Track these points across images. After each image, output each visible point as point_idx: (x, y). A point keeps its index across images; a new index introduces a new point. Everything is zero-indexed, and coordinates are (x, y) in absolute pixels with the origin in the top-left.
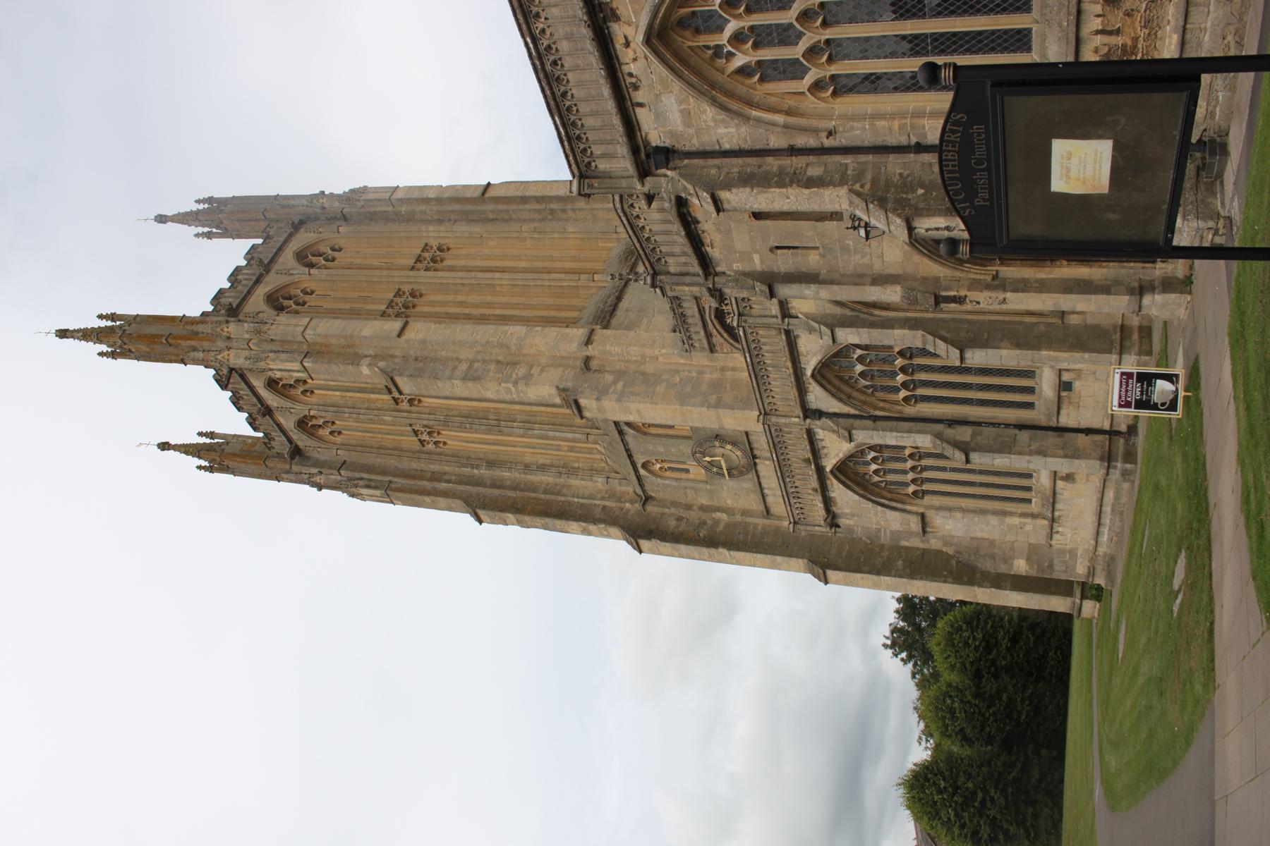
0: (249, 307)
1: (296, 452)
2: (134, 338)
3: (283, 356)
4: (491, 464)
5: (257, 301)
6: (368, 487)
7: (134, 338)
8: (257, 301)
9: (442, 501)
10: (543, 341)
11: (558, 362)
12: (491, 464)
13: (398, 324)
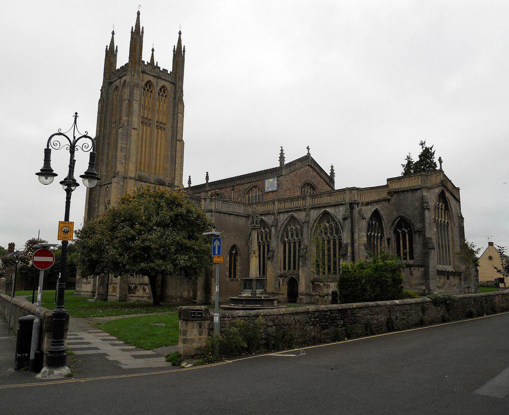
0: (145, 76)
1: (111, 83)
2: (137, 37)
3: (128, 94)
4: (108, 143)
5: (147, 78)
6: (101, 107)
7: (137, 37)
8: (147, 78)
9: (98, 129)
10: (132, 167)
11: (126, 171)
12: (108, 143)
13: (136, 127)
